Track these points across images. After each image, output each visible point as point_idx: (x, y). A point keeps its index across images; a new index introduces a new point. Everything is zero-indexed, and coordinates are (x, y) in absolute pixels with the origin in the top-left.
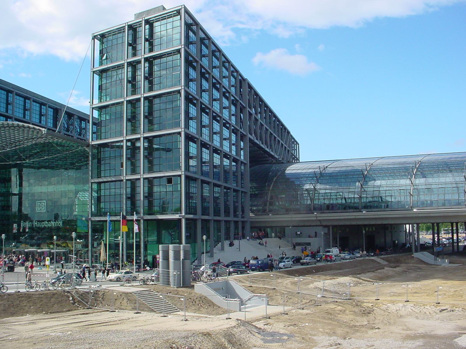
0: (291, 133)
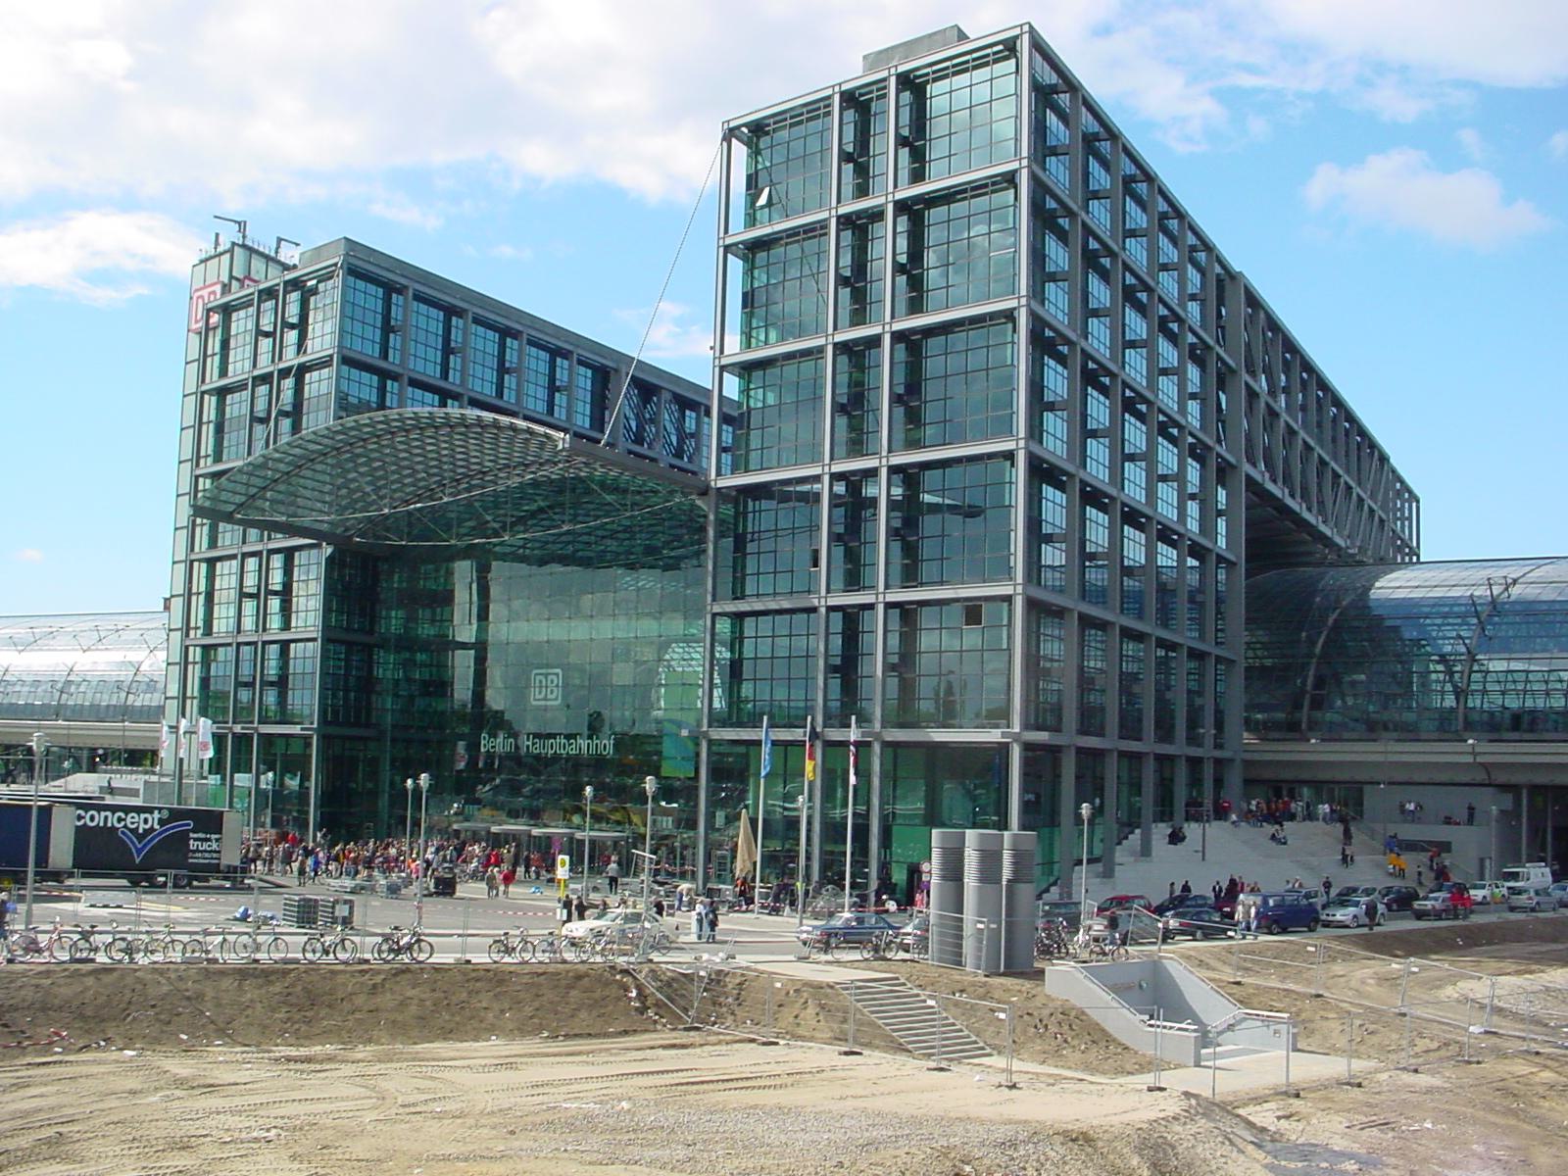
0: (1392, 461)
